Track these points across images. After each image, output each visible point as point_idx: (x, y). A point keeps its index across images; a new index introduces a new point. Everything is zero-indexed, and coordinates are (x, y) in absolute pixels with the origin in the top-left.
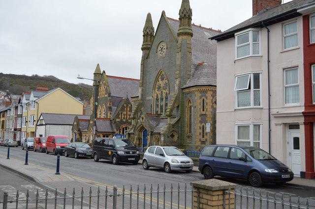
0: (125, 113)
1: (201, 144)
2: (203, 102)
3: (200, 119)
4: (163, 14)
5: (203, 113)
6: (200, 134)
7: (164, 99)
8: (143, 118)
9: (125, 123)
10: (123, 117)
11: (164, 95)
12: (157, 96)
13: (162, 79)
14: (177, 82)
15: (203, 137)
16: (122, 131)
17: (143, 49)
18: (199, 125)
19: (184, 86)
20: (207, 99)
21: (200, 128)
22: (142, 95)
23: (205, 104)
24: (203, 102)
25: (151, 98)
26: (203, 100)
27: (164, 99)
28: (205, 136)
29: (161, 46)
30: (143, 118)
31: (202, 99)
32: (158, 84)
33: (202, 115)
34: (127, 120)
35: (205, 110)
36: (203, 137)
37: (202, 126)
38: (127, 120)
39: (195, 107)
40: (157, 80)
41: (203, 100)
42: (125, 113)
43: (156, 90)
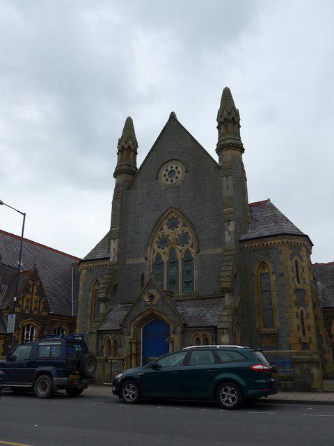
0: (29, 297)
1: (303, 348)
2: (297, 266)
3: (295, 298)
4: (173, 116)
5: (299, 286)
6: (299, 329)
7: (180, 263)
8: (152, 297)
9: (27, 316)
10: (25, 304)
11: (179, 256)
12: (159, 257)
13: (173, 225)
14: (231, 227)
15: (304, 333)
16: (21, 333)
17: (115, 175)
18: (295, 309)
19: (243, 237)
20: (302, 260)
21: (297, 317)
22: (119, 255)
23: (300, 271)
24: (297, 266)
25: (142, 260)
26: (296, 262)
27: (180, 263)
28: (307, 332)
29: (174, 166)
30: (152, 297)
31: (294, 261)
32: (159, 234)
33: (297, 290)
34: (31, 311)
35: (301, 281)
36: (304, 333)
37: (299, 311)
38: (31, 311)
39: (282, 275)
40: (158, 225)
41: (296, 262)
42: (29, 297)
43: (155, 246)
